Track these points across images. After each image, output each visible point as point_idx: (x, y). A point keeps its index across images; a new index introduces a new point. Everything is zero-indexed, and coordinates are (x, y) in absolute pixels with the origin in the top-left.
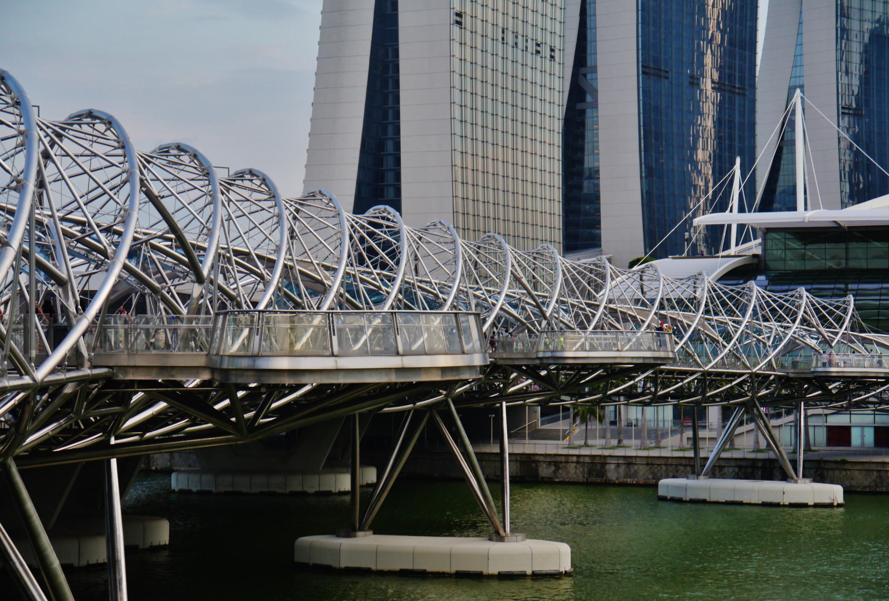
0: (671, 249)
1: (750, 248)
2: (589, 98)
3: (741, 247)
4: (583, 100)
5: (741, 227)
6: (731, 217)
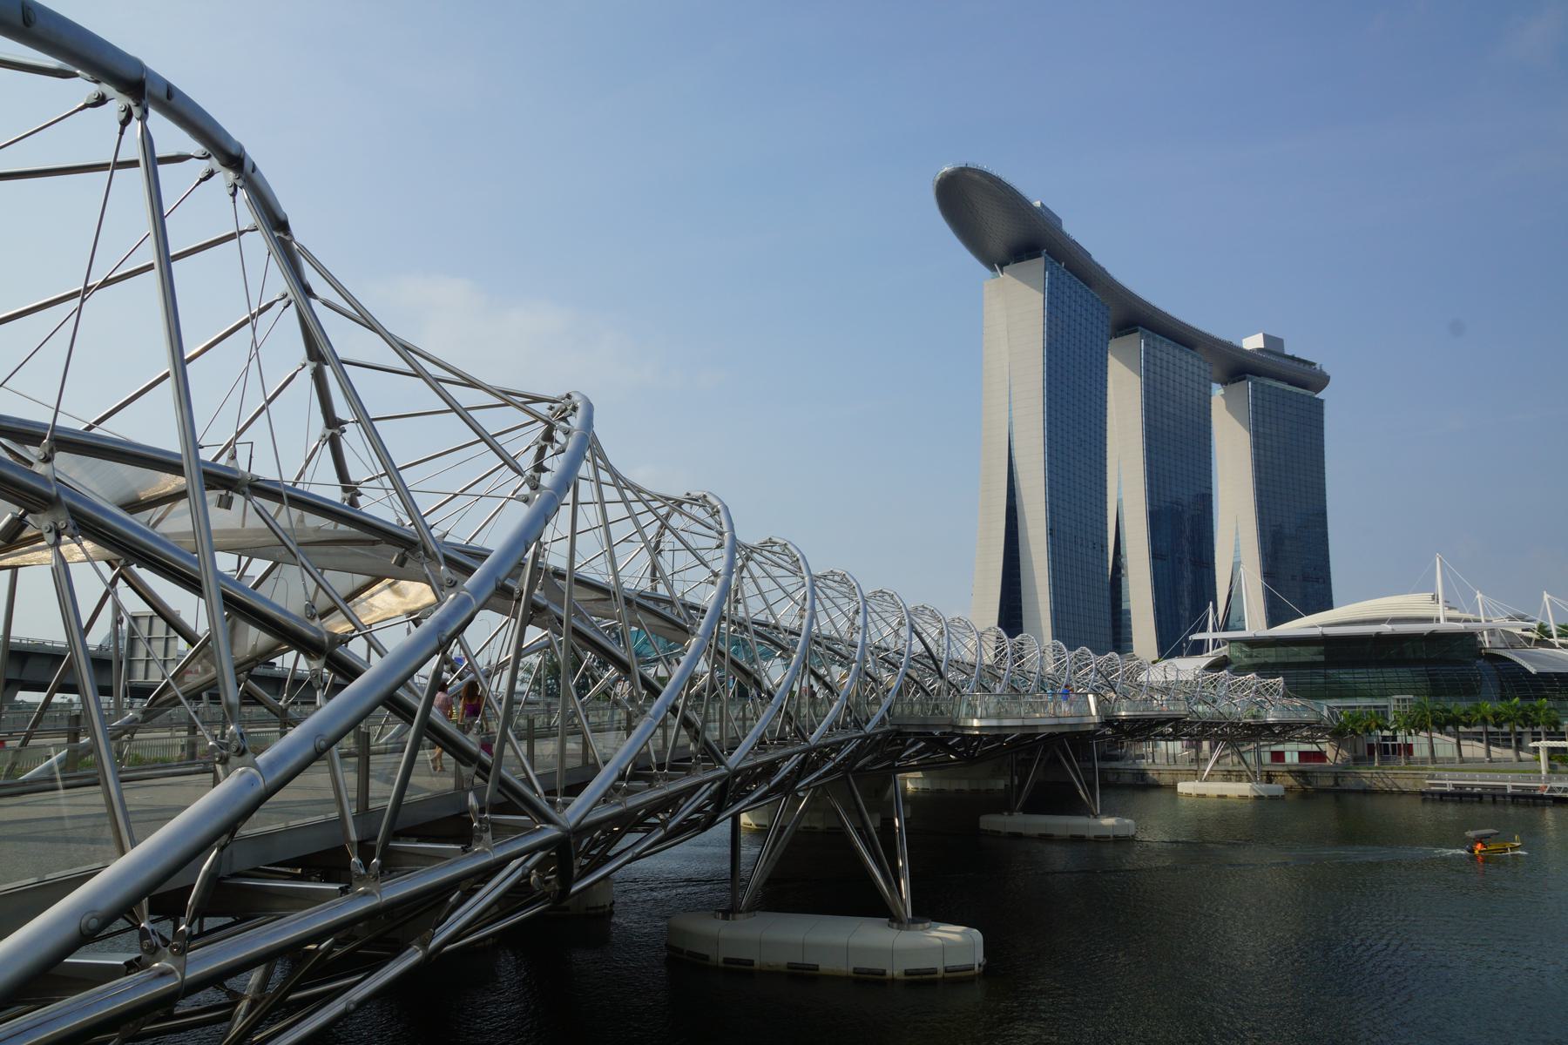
0: (1178, 653)
1: (1221, 652)
2: (1123, 572)
3: (1215, 651)
4: (1120, 572)
5: (1215, 640)
6: (1209, 635)
